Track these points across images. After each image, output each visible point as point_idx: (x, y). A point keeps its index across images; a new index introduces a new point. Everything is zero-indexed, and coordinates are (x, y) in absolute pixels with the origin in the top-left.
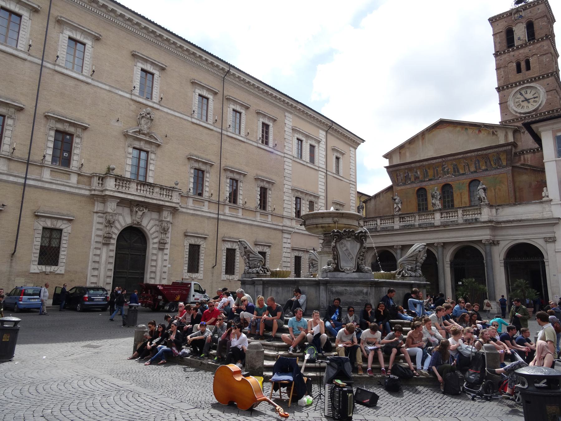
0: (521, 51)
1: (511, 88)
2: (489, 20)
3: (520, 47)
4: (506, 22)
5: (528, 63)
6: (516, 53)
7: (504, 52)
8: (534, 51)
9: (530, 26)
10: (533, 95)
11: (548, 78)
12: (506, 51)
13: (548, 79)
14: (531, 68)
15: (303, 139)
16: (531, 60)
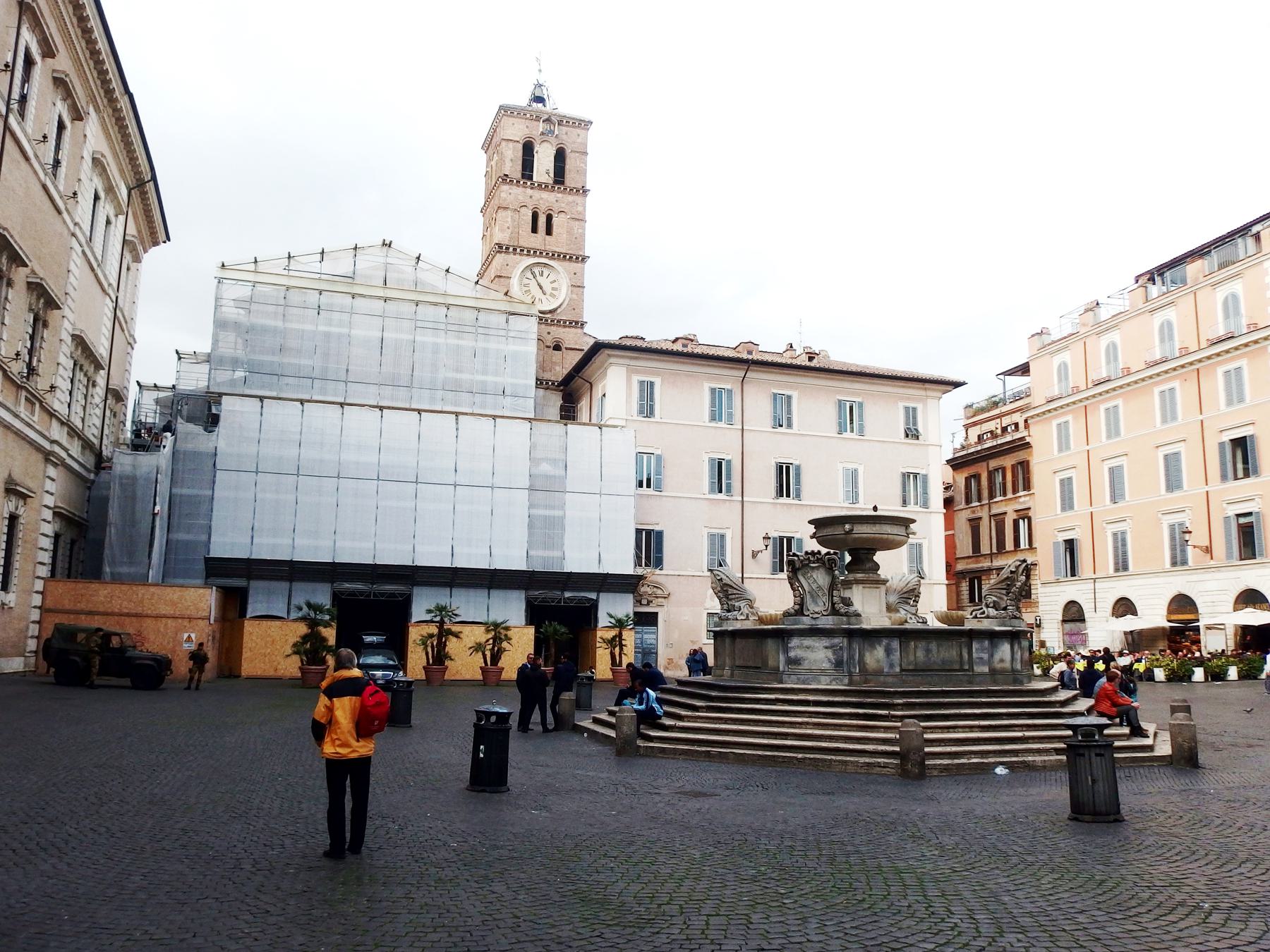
0: (545, 195)
1: (520, 255)
2: (501, 108)
3: (543, 186)
4: (527, 127)
5: (549, 218)
6: (537, 194)
7: (518, 182)
8: (563, 205)
9: (560, 156)
10: (551, 283)
11: (577, 262)
12: (522, 182)
13: (575, 264)
14: (554, 233)
15: (102, 194)
16: (555, 220)
